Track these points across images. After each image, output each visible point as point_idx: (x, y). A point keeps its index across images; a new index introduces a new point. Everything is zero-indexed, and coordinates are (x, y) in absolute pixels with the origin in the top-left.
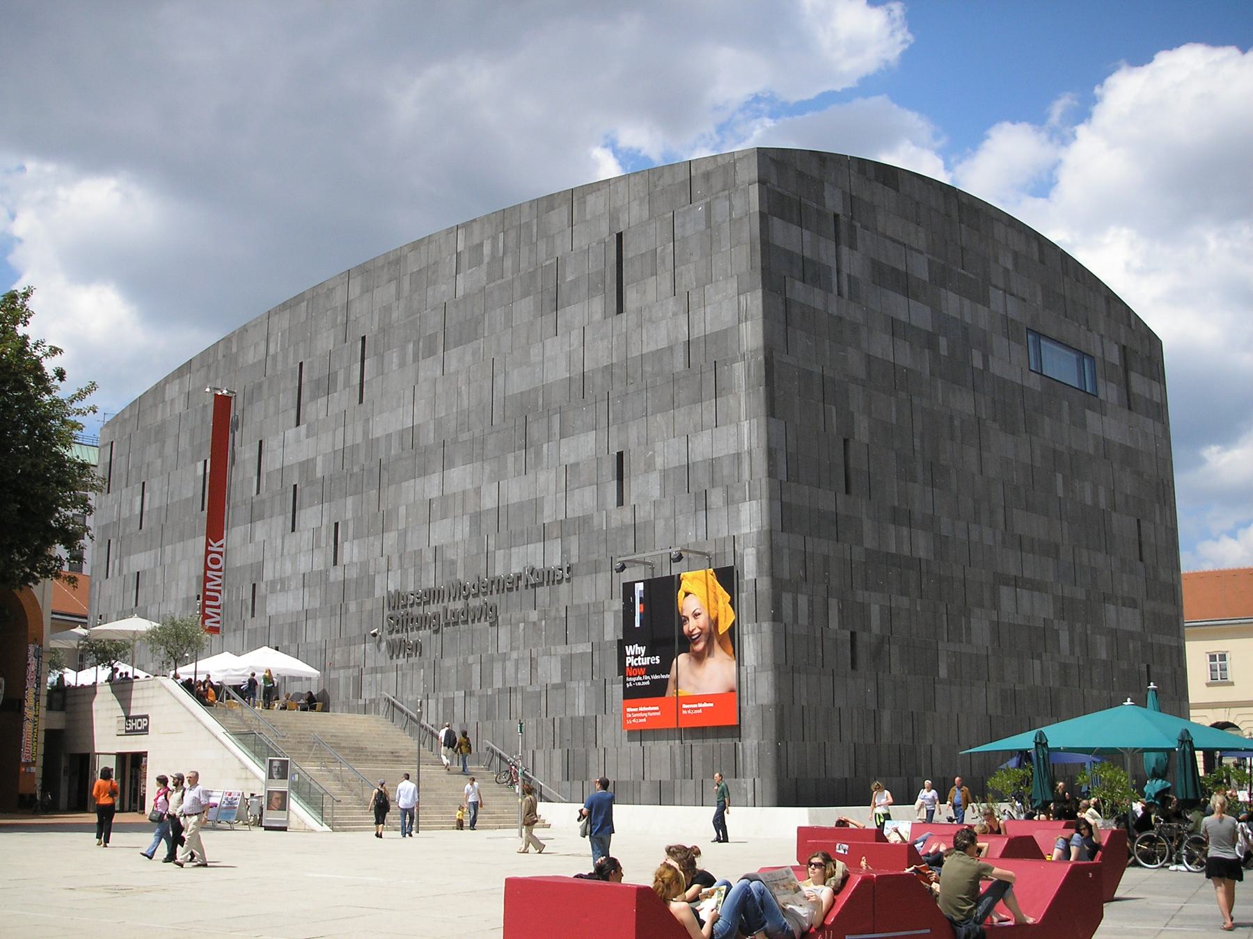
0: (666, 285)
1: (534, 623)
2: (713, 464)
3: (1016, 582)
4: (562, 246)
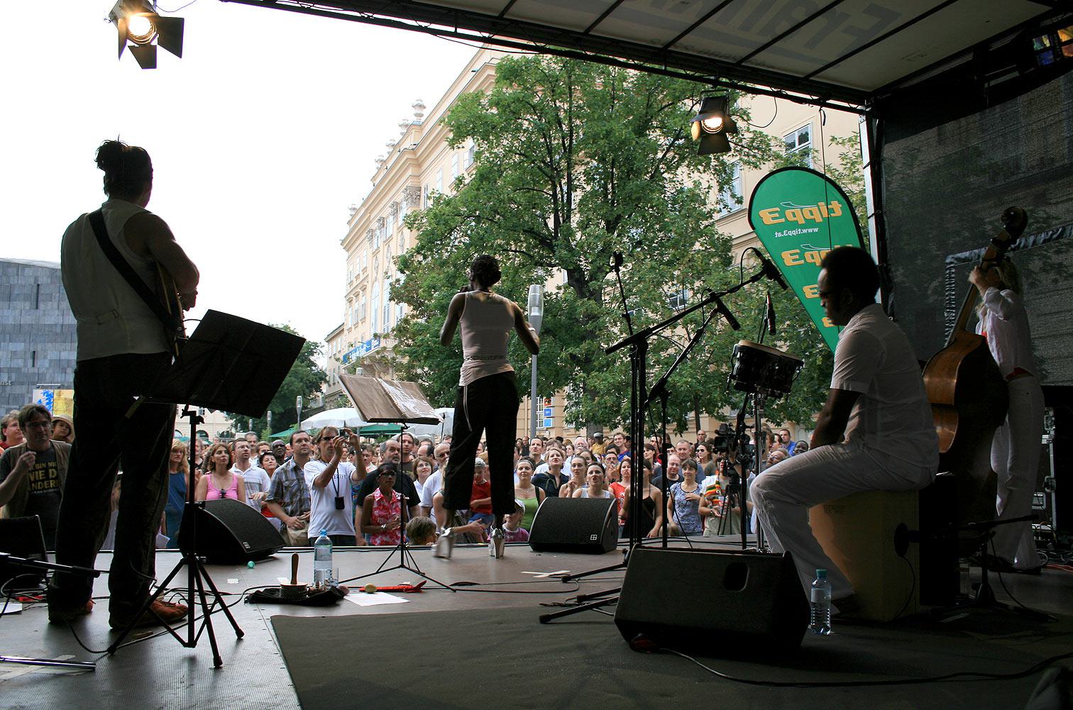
4: (13, 281)
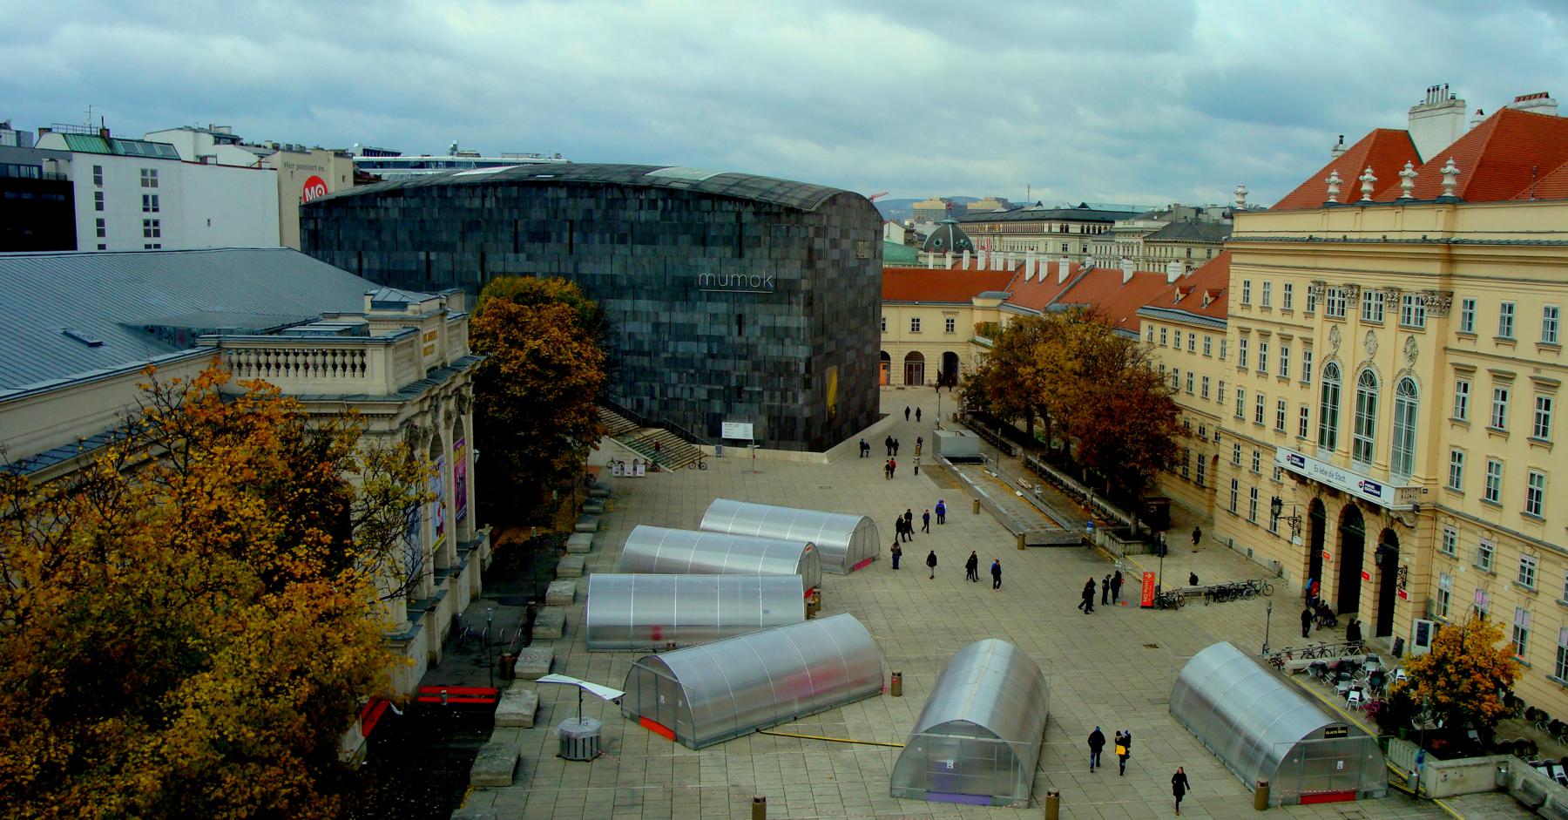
0: (766, 253)
2: (787, 329)
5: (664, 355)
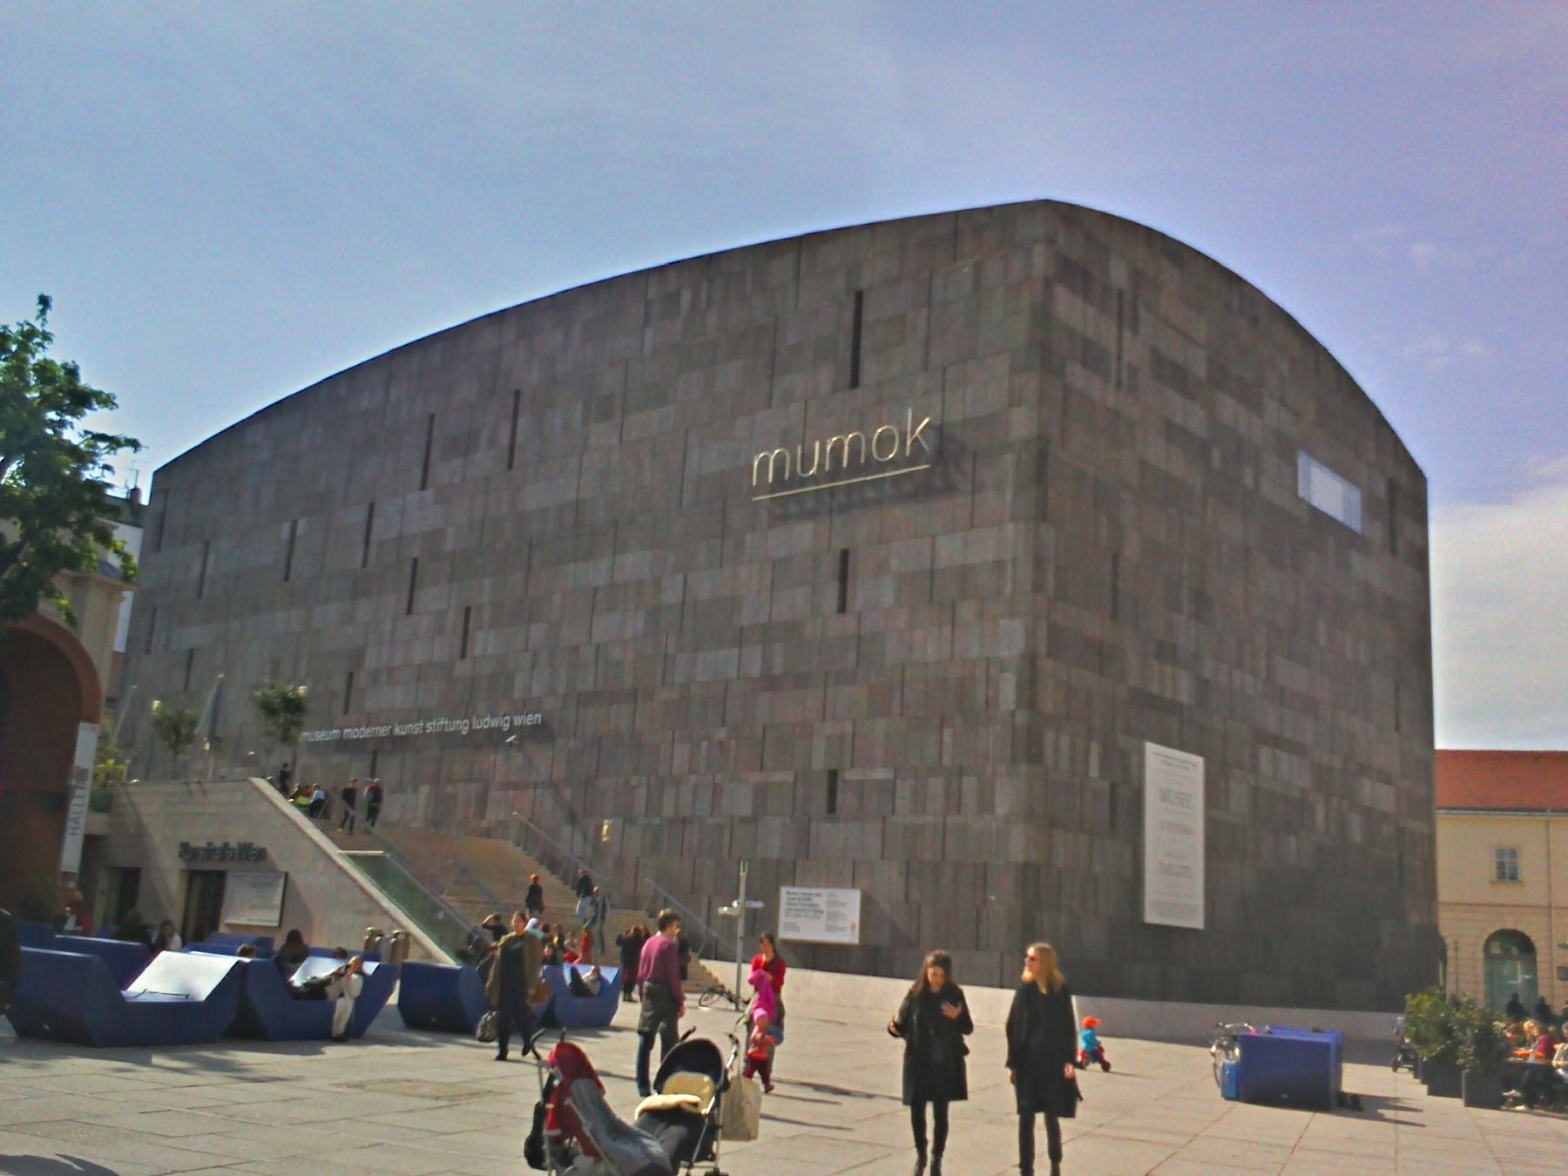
1: (721, 743)
2: (964, 573)
3: (1277, 742)
5: (664, 694)
